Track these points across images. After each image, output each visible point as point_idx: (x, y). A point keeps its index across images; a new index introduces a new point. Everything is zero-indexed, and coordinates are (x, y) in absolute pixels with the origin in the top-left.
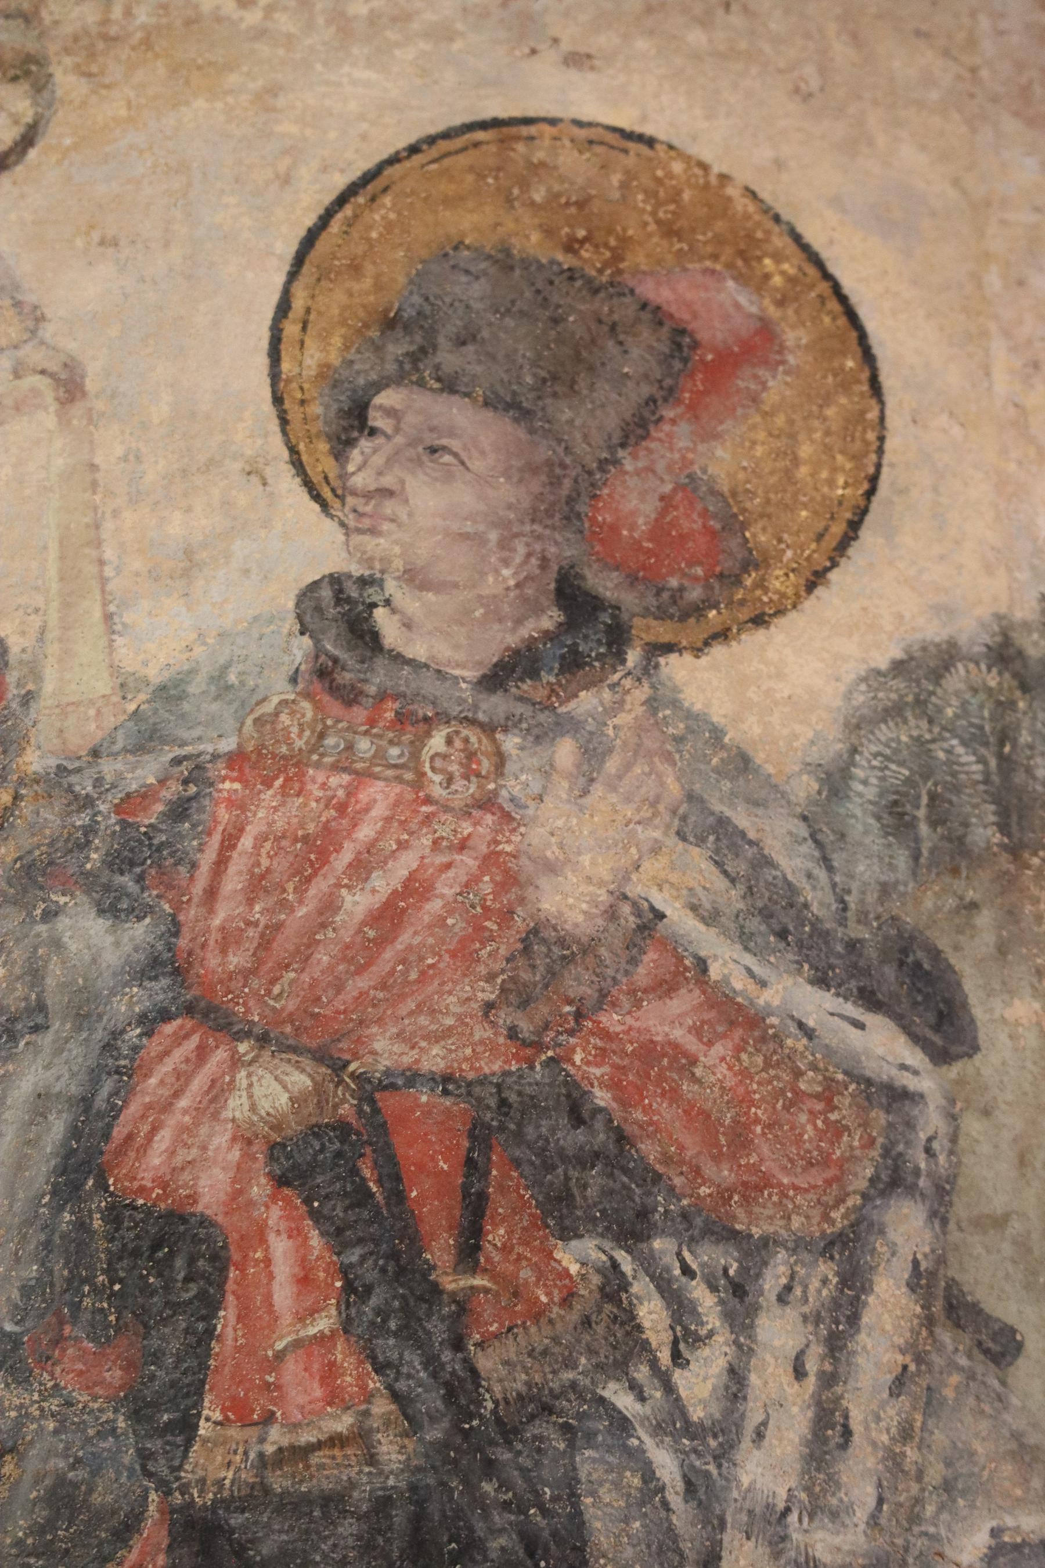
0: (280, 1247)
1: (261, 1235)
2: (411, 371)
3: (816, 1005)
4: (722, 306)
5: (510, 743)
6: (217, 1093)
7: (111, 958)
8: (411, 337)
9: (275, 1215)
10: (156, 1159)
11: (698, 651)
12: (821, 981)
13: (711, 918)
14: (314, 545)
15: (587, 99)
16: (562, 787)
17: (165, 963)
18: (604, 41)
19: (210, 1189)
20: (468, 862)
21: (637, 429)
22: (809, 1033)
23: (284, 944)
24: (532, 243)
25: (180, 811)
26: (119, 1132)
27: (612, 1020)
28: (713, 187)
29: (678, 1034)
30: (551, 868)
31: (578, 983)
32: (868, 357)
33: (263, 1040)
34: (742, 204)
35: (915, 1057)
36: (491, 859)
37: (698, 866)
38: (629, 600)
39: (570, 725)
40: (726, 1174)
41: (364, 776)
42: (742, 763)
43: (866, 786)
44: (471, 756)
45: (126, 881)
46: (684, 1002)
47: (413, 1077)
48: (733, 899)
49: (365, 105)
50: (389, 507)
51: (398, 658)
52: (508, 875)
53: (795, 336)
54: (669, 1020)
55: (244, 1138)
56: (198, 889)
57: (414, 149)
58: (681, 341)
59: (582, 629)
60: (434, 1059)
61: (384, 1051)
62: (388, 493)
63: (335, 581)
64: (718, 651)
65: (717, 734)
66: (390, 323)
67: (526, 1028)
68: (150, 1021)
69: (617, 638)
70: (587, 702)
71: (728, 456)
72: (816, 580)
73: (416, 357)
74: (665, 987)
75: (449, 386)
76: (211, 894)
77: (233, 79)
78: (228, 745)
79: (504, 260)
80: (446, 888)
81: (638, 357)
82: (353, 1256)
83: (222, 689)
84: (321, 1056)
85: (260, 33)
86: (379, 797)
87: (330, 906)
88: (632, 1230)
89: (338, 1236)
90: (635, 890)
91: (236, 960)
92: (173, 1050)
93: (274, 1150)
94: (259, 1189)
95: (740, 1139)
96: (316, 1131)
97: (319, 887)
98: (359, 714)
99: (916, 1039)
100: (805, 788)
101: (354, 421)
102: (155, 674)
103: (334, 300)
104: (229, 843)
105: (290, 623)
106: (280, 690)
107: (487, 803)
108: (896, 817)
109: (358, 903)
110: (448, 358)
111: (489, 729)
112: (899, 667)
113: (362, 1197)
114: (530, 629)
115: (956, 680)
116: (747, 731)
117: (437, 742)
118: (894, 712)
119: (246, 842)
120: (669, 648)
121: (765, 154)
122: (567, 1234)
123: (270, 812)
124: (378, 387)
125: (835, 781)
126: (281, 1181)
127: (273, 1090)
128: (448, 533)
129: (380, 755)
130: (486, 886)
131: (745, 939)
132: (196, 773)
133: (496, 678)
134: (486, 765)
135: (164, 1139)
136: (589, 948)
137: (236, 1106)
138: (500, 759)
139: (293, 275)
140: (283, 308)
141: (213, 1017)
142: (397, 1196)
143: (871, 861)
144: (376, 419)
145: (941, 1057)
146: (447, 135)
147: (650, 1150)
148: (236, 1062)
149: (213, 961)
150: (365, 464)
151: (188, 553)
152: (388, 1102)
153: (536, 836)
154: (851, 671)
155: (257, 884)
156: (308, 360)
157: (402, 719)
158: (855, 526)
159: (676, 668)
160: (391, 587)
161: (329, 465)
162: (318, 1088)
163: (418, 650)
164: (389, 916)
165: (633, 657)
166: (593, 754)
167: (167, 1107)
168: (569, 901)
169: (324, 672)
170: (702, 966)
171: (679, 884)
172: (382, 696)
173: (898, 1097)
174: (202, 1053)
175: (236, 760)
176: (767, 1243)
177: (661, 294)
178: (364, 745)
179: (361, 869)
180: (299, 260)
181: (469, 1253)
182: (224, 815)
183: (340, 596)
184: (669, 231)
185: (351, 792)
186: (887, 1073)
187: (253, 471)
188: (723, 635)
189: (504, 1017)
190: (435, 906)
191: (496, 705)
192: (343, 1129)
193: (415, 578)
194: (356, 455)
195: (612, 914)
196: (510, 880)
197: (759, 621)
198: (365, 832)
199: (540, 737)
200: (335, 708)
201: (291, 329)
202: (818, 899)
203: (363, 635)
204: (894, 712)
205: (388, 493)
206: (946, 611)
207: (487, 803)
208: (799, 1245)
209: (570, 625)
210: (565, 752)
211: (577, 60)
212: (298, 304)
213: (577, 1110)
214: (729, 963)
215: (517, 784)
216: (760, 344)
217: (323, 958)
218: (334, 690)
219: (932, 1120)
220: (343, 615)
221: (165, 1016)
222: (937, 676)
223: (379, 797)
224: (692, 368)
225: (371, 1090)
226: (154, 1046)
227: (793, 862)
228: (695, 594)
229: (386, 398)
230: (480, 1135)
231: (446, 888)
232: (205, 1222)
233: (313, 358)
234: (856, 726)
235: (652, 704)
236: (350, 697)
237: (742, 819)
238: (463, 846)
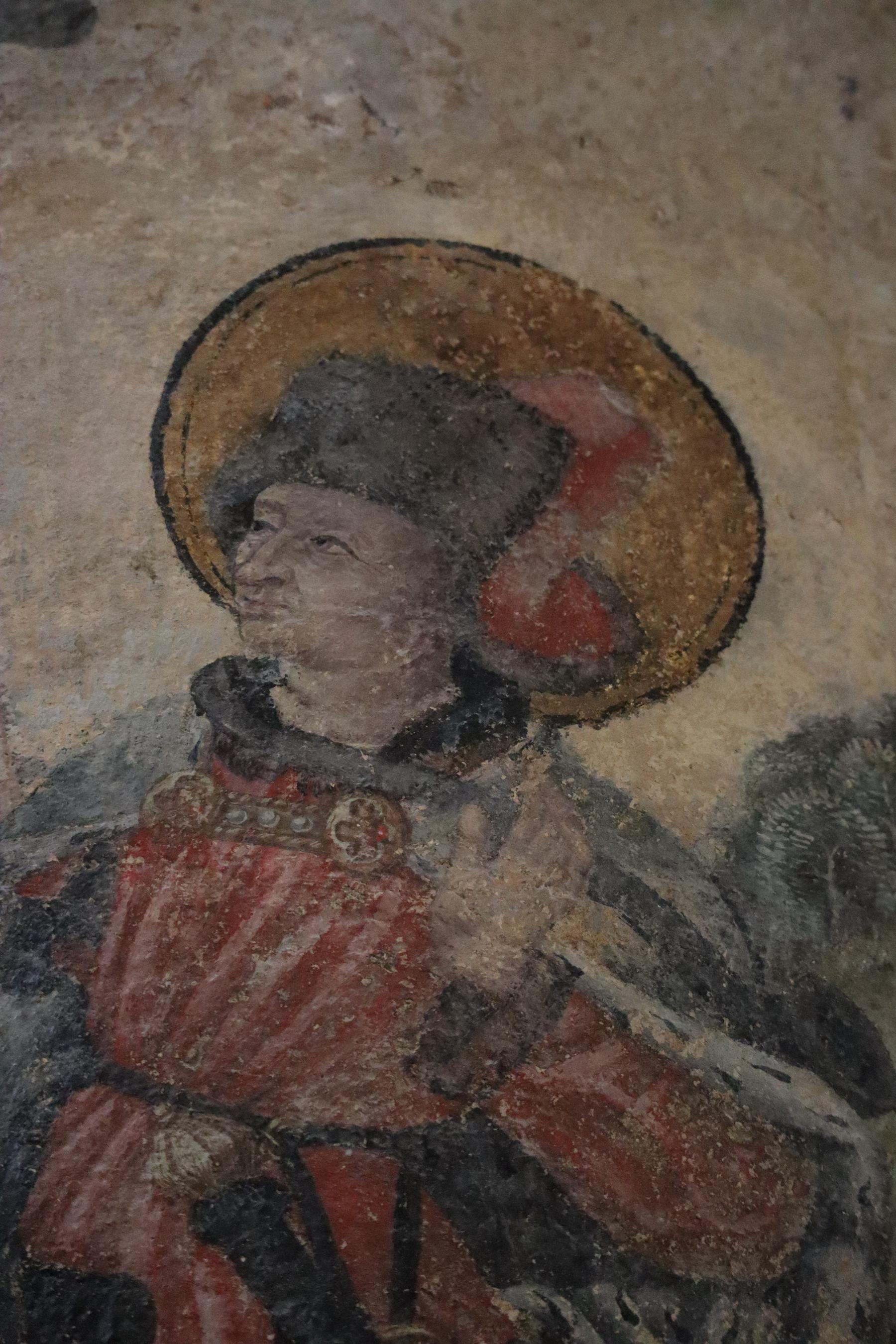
0: (207, 1302)
1: (187, 1290)
2: (296, 466)
3: (739, 1058)
4: (599, 407)
5: (416, 810)
6: (136, 1154)
7: (20, 1033)
8: (291, 440)
9: (201, 1272)
10: (74, 1224)
11: (597, 723)
12: (743, 1035)
13: (628, 975)
14: (206, 632)
15: (449, 221)
16: (470, 852)
17: (74, 1032)
18: (464, 171)
19: (133, 1248)
20: (380, 924)
21: (523, 518)
22: (735, 1085)
23: (199, 1006)
24: (405, 348)
25: (82, 888)
26: (35, 1198)
27: (535, 1073)
28: (581, 304)
29: (603, 1086)
30: (465, 929)
31: (499, 1037)
32: (743, 457)
33: (181, 1102)
34: (608, 317)
35: (840, 1109)
36: (403, 921)
37: (612, 923)
38: (525, 676)
39: (474, 793)
40: (661, 1221)
41: (269, 845)
42: (648, 826)
43: (772, 851)
44: (377, 823)
45: (33, 957)
46: (606, 1055)
47: (336, 1132)
48: (650, 955)
49: (236, 228)
50: (280, 594)
51: (300, 735)
52: (420, 935)
53: (670, 436)
54: (593, 1071)
55: (164, 1197)
56: (106, 960)
57: (284, 269)
58: (558, 440)
59: (478, 708)
60: (358, 1115)
61: (306, 1107)
62: (275, 581)
63: (231, 664)
64: (617, 723)
65: (621, 801)
66: (271, 425)
67: (448, 1080)
68: (61, 1092)
69: (516, 711)
70: (490, 771)
71: (613, 544)
72: (707, 658)
73: (299, 457)
74: (587, 1040)
75: (333, 481)
76: (119, 966)
77: (102, 212)
78: (129, 821)
79: (381, 367)
80: (359, 949)
81: (517, 456)
82: (285, 1309)
83: (119, 768)
84: (240, 1115)
85: (125, 170)
86: (286, 864)
87: (241, 970)
88: (571, 1275)
89: (268, 1291)
90: (551, 948)
91: (146, 1027)
92: (89, 1117)
93: (197, 1209)
94: (183, 1248)
95: (673, 1188)
96: (240, 1187)
97: (229, 954)
98: (262, 787)
99: (840, 1091)
100: (712, 851)
101: (241, 515)
102: (51, 757)
103: (215, 406)
104: (136, 911)
105: (186, 705)
106: (179, 768)
107: (394, 868)
108: (805, 880)
109: (269, 968)
110: (331, 458)
111: (394, 798)
112: (795, 741)
113: (291, 1249)
114: (428, 703)
115: (853, 753)
116: (653, 796)
117: (342, 812)
118: (794, 782)
119: (153, 913)
120: (568, 720)
121: (627, 272)
122: (503, 1281)
123: (172, 885)
124: (261, 485)
125: (742, 843)
126: (206, 1238)
127: (192, 1149)
128: (341, 620)
129: (284, 824)
130: (400, 948)
131: (664, 995)
132: (99, 851)
133: (398, 750)
134: (392, 832)
135: (82, 1203)
136: (507, 1004)
137: (155, 1167)
138: (407, 827)
139: (170, 386)
140: (163, 415)
141: (127, 1082)
142: (328, 1249)
143: (783, 921)
144: (263, 516)
145: (868, 1110)
146: (316, 255)
147: (583, 1198)
148: (153, 1125)
149: (124, 1029)
150: (252, 556)
151: (80, 645)
152: (313, 1158)
153: (448, 898)
154: (749, 743)
155: (165, 955)
156: (191, 462)
157: (304, 789)
158: (742, 610)
159: (577, 738)
160: (286, 667)
161: (218, 559)
162: (239, 1146)
163: (319, 727)
164: (303, 979)
165: (533, 729)
166: (500, 822)
167: (83, 1173)
168: (484, 959)
169: (223, 748)
170: (622, 1020)
171: (593, 946)
172: (284, 770)
173: (826, 1148)
174: (117, 1119)
175: (138, 836)
176: (708, 1289)
177: (539, 398)
178: (268, 815)
179: (270, 935)
180: (176, 372)
181: (404, 1301)
182: (128, 888)
183: (235, 679)
184: (539, 339)
185: (257, 860)
186: (816, 1124)
187: (142, 565)
188: (620, 708)
189: (425, 1071)
190: (348, 968)
191: (397, 776)
192: (267, 1184)
193: (308, 658)
194: (243, 548)
195: (528, 972)
196: (423, 940)
197: (656, 695)
198: (273, 899)
199: (444, 804)
200: (237, 782)
201: (172, 436)
202: (732, 957)
203: (261, 713)
204: (794, 782)
205: (275, 581)
206: (838, 690)
207: (394, 868)
208: (740, 1291)
209: (468, 699)
210: (471, 818)
211: (440, 188)
212: (178, 414)
213: (506, 1159)
214: (649, 1017)
215: (425, 849)
216: (637, 443)
217: (236, 1020)
218: (237, 766)
219: (864, 1171)
220: (239, 696)
221: (79, 1085)
222: (835, 748)
223: (286, 864)
224: (570, 467)
225: (291, 1145)
226: (67, 1114)
227: (707, 923)
228: (590, 670)
229: (272, 494)
230: (407, 1186)
231: (359, 949)
232: (130, 1283)
233: (195, 459)
234: (760, 794)
235: (556, 772)
236: (253, 771)
237: (652, 880)
238: (373, 909)
